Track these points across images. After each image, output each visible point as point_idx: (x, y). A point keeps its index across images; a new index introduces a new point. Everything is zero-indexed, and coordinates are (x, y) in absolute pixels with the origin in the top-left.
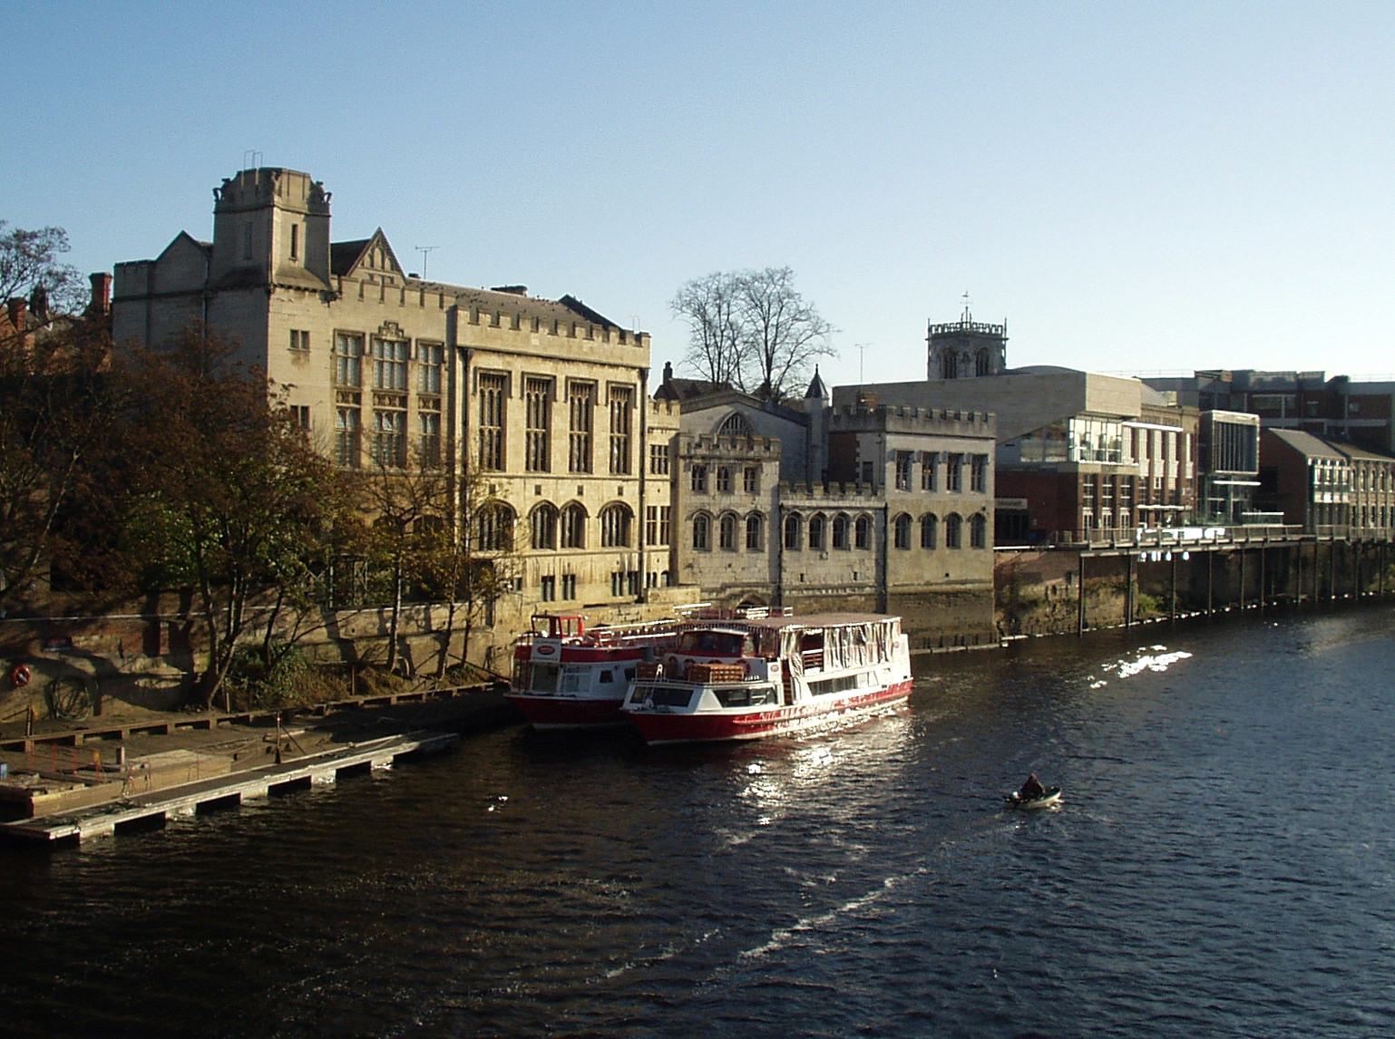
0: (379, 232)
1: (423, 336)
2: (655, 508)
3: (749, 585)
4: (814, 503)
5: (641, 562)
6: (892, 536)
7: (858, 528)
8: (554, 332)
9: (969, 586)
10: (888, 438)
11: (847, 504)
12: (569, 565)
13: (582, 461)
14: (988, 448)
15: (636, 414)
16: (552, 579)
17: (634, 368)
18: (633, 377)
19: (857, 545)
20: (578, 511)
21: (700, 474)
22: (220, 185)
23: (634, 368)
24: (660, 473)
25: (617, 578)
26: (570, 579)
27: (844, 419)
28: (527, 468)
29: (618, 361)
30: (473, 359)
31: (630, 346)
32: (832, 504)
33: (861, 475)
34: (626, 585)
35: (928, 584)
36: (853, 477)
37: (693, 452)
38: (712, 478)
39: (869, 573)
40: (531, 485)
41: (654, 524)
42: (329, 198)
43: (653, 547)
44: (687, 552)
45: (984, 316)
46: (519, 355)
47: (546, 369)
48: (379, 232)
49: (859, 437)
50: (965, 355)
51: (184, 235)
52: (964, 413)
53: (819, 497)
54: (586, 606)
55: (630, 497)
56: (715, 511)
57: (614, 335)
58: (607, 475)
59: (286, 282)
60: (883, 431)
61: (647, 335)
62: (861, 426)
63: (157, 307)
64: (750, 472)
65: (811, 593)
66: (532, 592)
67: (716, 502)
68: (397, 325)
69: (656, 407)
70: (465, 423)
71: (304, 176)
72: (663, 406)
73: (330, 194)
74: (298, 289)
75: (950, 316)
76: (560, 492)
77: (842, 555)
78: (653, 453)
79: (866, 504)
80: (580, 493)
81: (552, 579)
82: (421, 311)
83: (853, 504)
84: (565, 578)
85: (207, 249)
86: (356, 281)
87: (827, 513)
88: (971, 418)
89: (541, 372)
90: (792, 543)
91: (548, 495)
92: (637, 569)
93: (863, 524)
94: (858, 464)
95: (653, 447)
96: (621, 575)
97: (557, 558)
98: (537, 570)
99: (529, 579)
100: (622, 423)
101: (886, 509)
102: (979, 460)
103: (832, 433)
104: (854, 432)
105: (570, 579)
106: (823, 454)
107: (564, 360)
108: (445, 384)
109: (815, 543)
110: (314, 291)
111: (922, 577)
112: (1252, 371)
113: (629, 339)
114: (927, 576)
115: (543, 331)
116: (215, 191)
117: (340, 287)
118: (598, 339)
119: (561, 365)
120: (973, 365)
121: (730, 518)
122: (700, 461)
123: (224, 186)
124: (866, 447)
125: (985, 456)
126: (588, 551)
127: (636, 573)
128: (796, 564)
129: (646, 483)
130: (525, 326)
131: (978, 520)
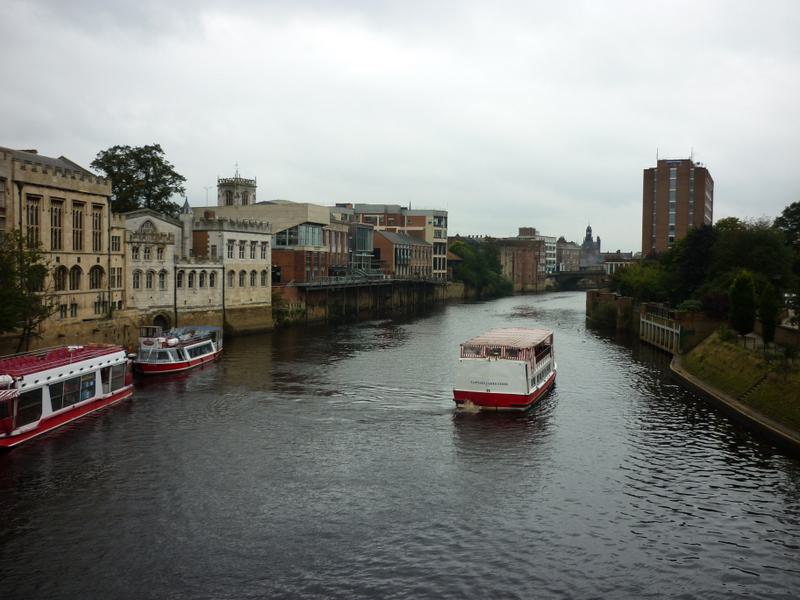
4: (189, 266)
9: (261, 305)
10: (225, 233)
13: (78, 244)
14: (268, 238)
16: (66, 306)
17: (104, 196)
18: (104, 201)
20: (77, 270)
21: (135, 250)
23: (104, 196)
25: (97, 305)
26: (74, 306)
27: (201, 223)
34: (101, 309)
38: (142, 253)
39: (217, 300)
44: (130, 291)
45: (245, 176)
47: (60, 195)
50: (237, 194)
54: (85, 320)
55: (103, 262)
56: (144, 270)
57: (93, 179)
62: (209, 228)
67: (144, 266)
69: (114, 217)
72: (117, 216)
75: (230, 175)
76: (69, 262)
81: (66, 306)
84: (72, 305)
91: (63, 262)
93: (212, 276)
100: (97, 224)
102: (264, 243)
103: (194, 231)
104: (206, 231)
108: (8, 202)
109: (190, 285)
111: (239, 301)
114: (242, 301)
118: (86, 181)
119: (69, 194)
120: (241, 199)
121: (151, 273)
124: (213, 238)
125: (267, 242)
130: (50, 172)
131: (264, 273)
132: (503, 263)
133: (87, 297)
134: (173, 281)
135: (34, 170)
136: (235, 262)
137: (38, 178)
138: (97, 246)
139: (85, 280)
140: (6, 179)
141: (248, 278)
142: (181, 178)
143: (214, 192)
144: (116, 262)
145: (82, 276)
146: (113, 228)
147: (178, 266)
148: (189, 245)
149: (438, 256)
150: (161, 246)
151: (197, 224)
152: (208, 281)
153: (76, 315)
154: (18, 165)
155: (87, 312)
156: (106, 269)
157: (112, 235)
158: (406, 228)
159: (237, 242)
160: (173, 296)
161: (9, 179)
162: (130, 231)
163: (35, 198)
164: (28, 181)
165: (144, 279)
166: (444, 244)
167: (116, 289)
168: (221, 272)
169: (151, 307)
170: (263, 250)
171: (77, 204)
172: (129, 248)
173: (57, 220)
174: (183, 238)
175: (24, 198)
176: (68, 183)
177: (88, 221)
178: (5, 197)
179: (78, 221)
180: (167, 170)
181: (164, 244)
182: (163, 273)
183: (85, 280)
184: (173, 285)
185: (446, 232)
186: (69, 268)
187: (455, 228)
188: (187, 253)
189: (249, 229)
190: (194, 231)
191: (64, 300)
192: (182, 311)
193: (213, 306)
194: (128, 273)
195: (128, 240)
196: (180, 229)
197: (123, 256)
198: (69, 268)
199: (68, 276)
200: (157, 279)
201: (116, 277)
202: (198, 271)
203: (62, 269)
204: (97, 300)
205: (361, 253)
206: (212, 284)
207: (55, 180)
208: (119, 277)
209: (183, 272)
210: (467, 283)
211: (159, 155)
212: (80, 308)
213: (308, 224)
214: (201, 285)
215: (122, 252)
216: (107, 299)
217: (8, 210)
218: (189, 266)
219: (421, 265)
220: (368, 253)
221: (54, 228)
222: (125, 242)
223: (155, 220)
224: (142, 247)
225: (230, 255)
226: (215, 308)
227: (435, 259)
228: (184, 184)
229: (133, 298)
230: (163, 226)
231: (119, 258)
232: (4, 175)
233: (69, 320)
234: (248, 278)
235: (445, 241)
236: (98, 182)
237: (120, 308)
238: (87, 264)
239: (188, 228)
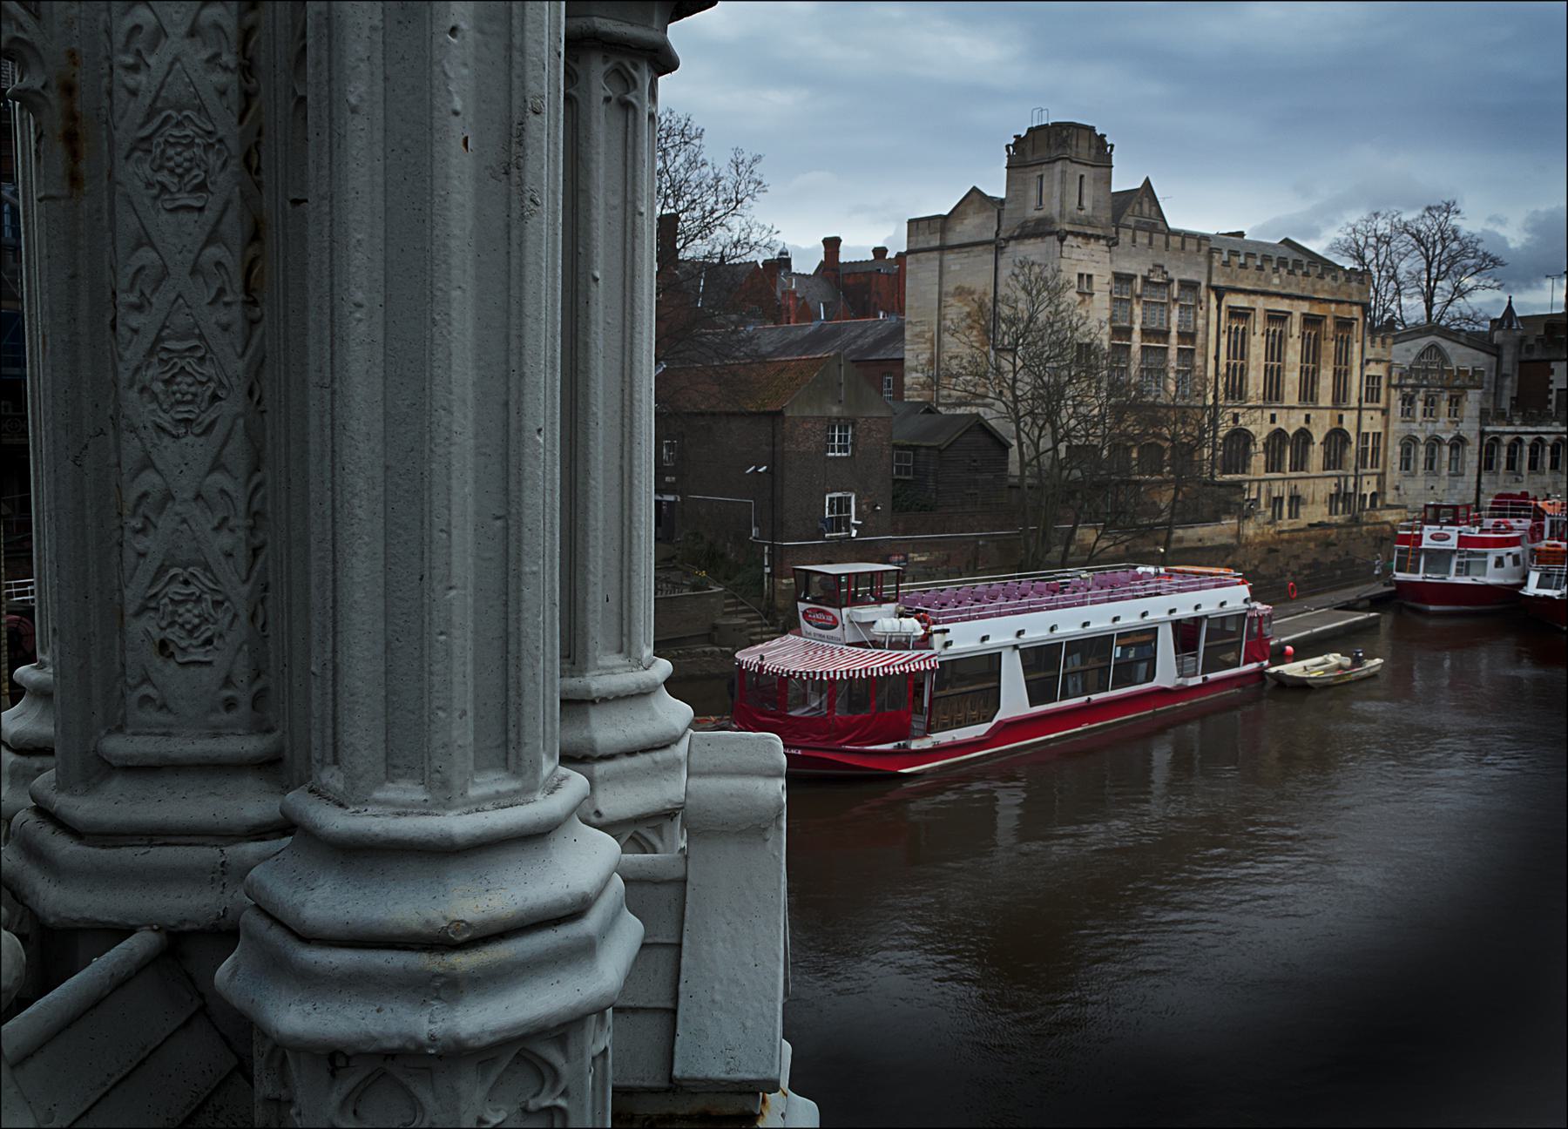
0: (1147, 182)
1: (1184, 277)
2: (1367, 434)
4: (1509, 429)
5: (1355, 485)
7: (1552, 452)
8: (1291, 273)
11: (1544, 429)
12: (1296, 487)
13: (1308, 393)
15: (1356, 348)
16: (1281, 499)
18: (1356, 311)
19: (1551, 468)
20: (1304, 436)
21: (1408, 400)
22: (1012, 141)
24: (1372, 401)
25: (1333, 499)
26: (1296, 500)
29: (1344, 298)
30: (1225, 298)
32: (1530, 429)
33: (1554, 402)
34: (1340, 505)
37: (1403, 382)
38: (1420, 406)
40: (1267, 414)
41: (1367, 449)
42: (1111, 150)
43: (1365, 471)
44: (1394, 474)
47: (1283, 305)
48: (1147, 182)
49: (1553, 365)
53: (1518, 423)
56: (1422, 437)
63: (950, 257)
64: (1454, 400)
67: (1421, 429)
68: (1162, 267)
69: (1373, 342)
70: (1217, 358)
71: (1092, 129)
73: (1112, 146)
76: (1291, 422)
77: (1538, 478)
78: (1367, 383)
81: (1281, 499)
82: (1182, 255)
83: (1550, 429)
84: (1291, 498)
85: (1002, 201)
86: (1128, 227)
87: (1524, 437)
89: (1280, 309)
91: (1279, 424)
94: (1551, 392)
95: (1368, 377)
96: (1338, 494)
97: (1286, 482)
98: (1269, 492)
99: (1263, 501)
103: (1521, 362)
104: (1550, 361)
105: (1296, 500)
106: (1513, 381)
108: (1200, 322)
109: (1511, 465)
110: (1098, 238)
116: (1008, 147)
121: (1434, 442)
122: (1409, 390)
123: (1015, 143)
126: (1313, 474)
127: (1350, 494)
128: (1494, 486)
129: (1364, 413)
130: (1268, 268)
133: (1318, 487)
134: (1476, 458)
138: (1340, 396)
140: (1200, 284)
144: (1372, 423)
145: (1311, 448)
146: (1368, 361)
147: (1488, 429)
148: (1509, 388)
150: (1456, 392)
151: (1530, 349)
153: (1297, 517)
157: (1367, 373)
160: (1474, 486)
161: (1204, 284)
164: (1232, 285)
167: (1369, 470)
172: (1396, 395)
173: (1275, 349)
174: (1500, 376)
178: (1196, 314)
181: (1463, 388)
182: (1458, 443)
184: (1475, 464)
186: (1291, 433)
188: (1506, 404)
190: (1521, 362)
191: (1280, 489)
194: (1390, 442)
195: (1395, 381)
196: (1495, 359)
197: (1385, 412)
198: (1291, 433)
202: (1528, 439)
203: (1279, 434)
204: (1333, 490)
208: (1376, 450)
209: (1497, 440)
211: (1454, 221)
212: (1305, 503)
214: (1533, 465)
215: (1382, 405)
216: (1351, 489)
217: (1200, 337)
218: (1509, 429)
221: (1338, 367)
222: (1389, 386)
229: (1397, 488)
231: (1378, 415)
232: (1195, 278)
236: (1348, 280)
239: (1508, 357)
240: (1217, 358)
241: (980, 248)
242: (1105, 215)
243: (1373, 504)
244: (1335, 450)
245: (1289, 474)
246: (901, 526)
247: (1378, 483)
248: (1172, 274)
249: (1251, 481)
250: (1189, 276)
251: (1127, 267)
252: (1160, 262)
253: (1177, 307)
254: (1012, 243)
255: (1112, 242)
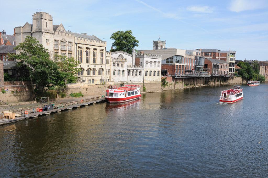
1: (69, 41)
3: (122, 81)
4: (132, 69)
5: (105, 78)
6: (145, 74)
7: (139, 73)
9: (157, 82)
13: (95, 61)
20: (94, 69)
21: (114, 63)
26: (93, 80)
28: (86, 63)
31: (103, 44)
32: (135, 69)
34: (102, 81)
35: (151, 82)
36: (139, 65)
38: (116, 64)
40: (87, 65)
46: (85, 44)
49: (140, 58)
51: (27, 23)
52: (157, 55)
55: (103, 67)
56: (117, 70)
58: (99, 64)
59: (45, 31)
60: (144, 58)
61: (106, 42)
65: (132, 83)
66: (87, 82)
67: (117, 68)
70: (76, 55)
71: (48, 14)
74: (47, 33)
75: (156, 40)
76: (92, 67)
79: (141, 69)
80: (95, 66)
87: (134, 70)
88: (158, 56)
90: (129, 75)
92: (104, 79)
93: (140, 72)
99: (87, 80)
100: (101, 55)
101: (144, 70)
107: (92, 45)
108: (73, 49)
109: (132, 75)
112: (205, 49)
113: (103, 42)
115: (89, 41)
117: (55, 33)
118: (98, 42)
130: (86, 40)
132: (260, 70)
135: (81, 40)
136: (148, 68)
137: (82, 42)
138: (101, 61)
139: (97, 72)
141: (152, 73)
142: (138, 42)
143: (152, 45)
144: (108, 67)
146: (107, 57)
147: (128, 69)
149: (231, 67)
152: (138, 73)
154: (76, 38)
155: (98, 82)
156: (104, 69)
158: (220, 57)
159: (149, 62)
161: (73, 42)
162: (112, 58)
163: (82, 48)
165: (117, 73)
166: (234, 63)
168: (143, 71)
169: (118, 81)
170: (159, 64)
171: (95, 49)
172: (112, 63)
173: (88, 54)
174: (132, 60)
175: (78, 48)
176: (92, 43)
177: (98, 55)
179: (95, 55)
180: (133, 38)
182: (123, 71)
183: (97, 72)
185: (234, 59)
186: (92, 69)
187: (239, 57)
188: (134, 65)
189: (154, 57)
190: (136, 58)
192: (129, 83)
193: (140, 82)
195: (112, 60)
198: (92, 69)
199: (91, 71)
200: (121, 73)
201: (108, 72)
202: (135, 71)
203: (90, 69)
205: (199, 66)
206: (140, 75)
207: (88, 42)
208: (109, 72)
210: (244, 78)
213: (176, 55)
214: (136, 75)
215: (110, 64)
216: (104, 78)
217: (73, 52)
219: (224, 70)
220: (203, 66)
223: (123, 54)
224: (116, 63)
225: (146, 66)
226: (141, 83)
227: (230, 69)
228: (138, 44)
230: (126, 56)
233: (91, 84)
234: (152, 73)
235: (234, 62)
237: (109, 81)
238: (98, 67)
239: (134, 57)
240: (76, 55)
241: (29, 33)
242: (51, 30)
243: (109, 81)
244: (101, 72)
245: (92, 76)
246: (6, 84)
247: (110, 77)
248: (66, 40)
249: (84, 77)
250: (70, 41)
251: (57, 39)
252: (64, 38)
253: (68, 46)
254: (34, 33)
255: (53, 34)
